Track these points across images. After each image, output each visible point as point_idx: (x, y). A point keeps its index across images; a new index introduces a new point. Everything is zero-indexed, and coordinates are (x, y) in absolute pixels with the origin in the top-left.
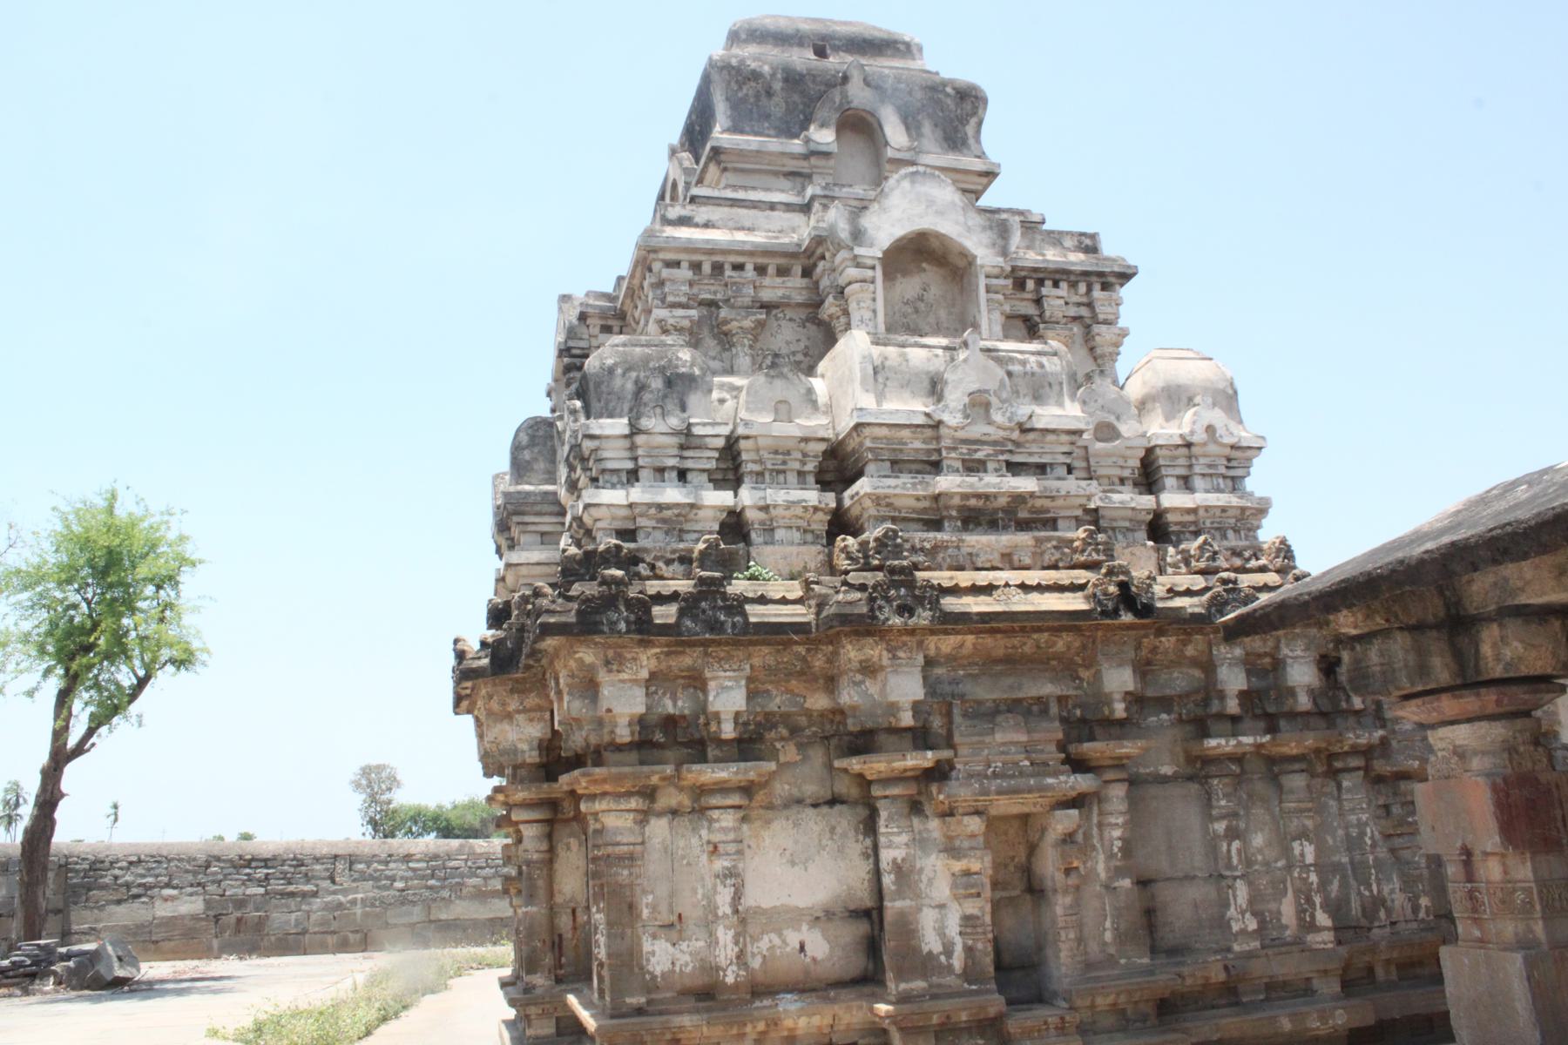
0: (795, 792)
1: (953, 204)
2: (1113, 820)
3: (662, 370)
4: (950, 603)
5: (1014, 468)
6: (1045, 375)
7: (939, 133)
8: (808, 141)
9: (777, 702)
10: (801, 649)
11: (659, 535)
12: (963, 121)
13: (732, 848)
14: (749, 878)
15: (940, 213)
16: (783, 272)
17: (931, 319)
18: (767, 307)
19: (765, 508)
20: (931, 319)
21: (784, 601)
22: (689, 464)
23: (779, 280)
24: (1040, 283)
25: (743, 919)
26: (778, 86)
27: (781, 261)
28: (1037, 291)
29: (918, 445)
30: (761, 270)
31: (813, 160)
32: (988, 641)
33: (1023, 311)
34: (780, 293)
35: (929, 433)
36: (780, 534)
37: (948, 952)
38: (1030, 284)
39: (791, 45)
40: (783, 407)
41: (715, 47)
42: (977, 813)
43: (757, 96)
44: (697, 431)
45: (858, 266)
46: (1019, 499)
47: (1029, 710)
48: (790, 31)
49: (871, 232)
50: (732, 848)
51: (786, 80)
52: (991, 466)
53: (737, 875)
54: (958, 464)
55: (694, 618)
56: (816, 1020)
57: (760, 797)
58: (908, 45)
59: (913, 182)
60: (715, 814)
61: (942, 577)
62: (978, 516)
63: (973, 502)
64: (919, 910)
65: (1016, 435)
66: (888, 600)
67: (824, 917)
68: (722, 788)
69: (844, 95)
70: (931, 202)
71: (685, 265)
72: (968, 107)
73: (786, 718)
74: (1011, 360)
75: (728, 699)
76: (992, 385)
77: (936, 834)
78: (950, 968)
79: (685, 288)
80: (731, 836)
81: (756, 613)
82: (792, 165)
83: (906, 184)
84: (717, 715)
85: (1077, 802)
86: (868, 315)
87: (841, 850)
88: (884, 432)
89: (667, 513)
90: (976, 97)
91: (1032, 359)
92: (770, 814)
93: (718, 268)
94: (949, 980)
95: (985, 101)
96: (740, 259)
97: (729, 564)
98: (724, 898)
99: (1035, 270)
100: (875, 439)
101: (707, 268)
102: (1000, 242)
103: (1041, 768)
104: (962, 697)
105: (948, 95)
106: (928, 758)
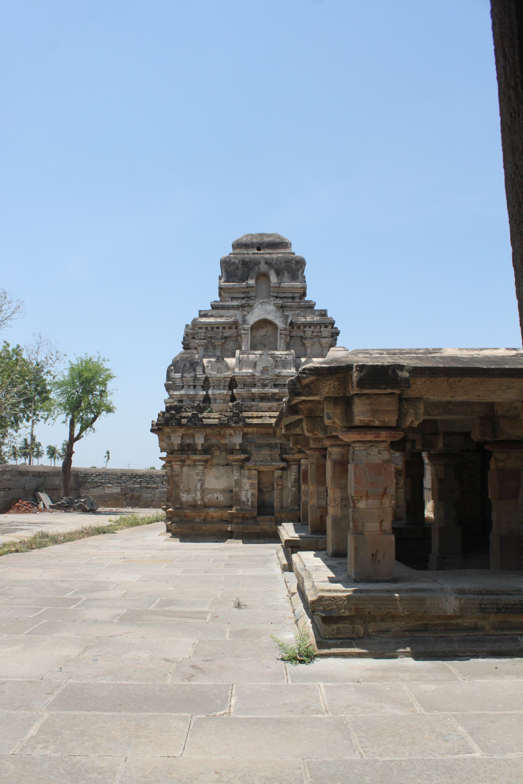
0: (218, 462)
1: (272, 310)
2: (292, 474)
3: (190, 361)
4: (248, 421)
5: (275, 386)
6: (287, 360)
7: (290, 275)
8: (247, 283)
9: (214, 441)
10: (218, 430)
11: (188, 401)
12: (298, 271)
13: (201, 474)
14: (206, 481)
15: (269, 313)
16: (230, 328)
17: (268, 341)
18: (226, 338)
19: (214, 395)
20: (268, 341)
21: (214, 418)
22: (196, 384)
23: (229, 330)
24: (305, 327)
25: (203, 491)
26: (240, 266)
27: (229, 326)
28: (304, 329)
29: (250, 380)
30: (224, 328)
31: (249, 288)
32: (260, 429)
33: (300, 335)
34: (229, 334)
35: (252, 377)
36: (218, 401)
37: (248, 501)
38: (302, 327)
39: (250, 248)
40: (220, 369)
41: (227, 251)
42: (256, 470)
43: (234, 270)
44: (198, 376)
45: (244, 330)
46: (274, 394)
47: (270, 446)
48: (250, 243)
49: (248, 320)
50: (201, 474)
51: (242, 264)
52: (269, 385)
53: (202, 480)
54: (260, 385)
55: (191, 422)
56: (217, 514)
57: (209, 463)
58: (287, 243)
59: (262, 305)
60: (198, 466)
61: (245, 414)
62: (264, 398)
63: (262, 395)
64: (241, 491)
65: (275, 377)
66: (232, 420)
67: (223, 491)
68: (199, 461)
69: (259, 268)
70: (266, 310)
71: (204, 328)
72: (299, 266)
73: (217, 445)
74: (278, 357)
75: (200, 440)
76: (269, 365)
77: (247, 474)
78: (248, 505)
79: (204, 335)
80: (201, 471)
81: (205, 421)
82: (243, 290)
83: (260, 306)
84: (197, 444)
85: (283, 469)
86: (246, 343)
87: (228, 476)
88: (241, 377)
89: (190, 396)
90: (302, 263)
91: (284, 356)
92: (212, 467)
93: (212, 328)
94: (247, 507)
95: (305, 264)
96: (218, 326)
97: (201, 410)
98: (199, 485)
99: (303, 324)
100: (238, 379)
101: (209, 329)
102: (285, 320)
103: (273, 460)
104: (255, 442)
105: (293, 263)
106: (243, 457)
